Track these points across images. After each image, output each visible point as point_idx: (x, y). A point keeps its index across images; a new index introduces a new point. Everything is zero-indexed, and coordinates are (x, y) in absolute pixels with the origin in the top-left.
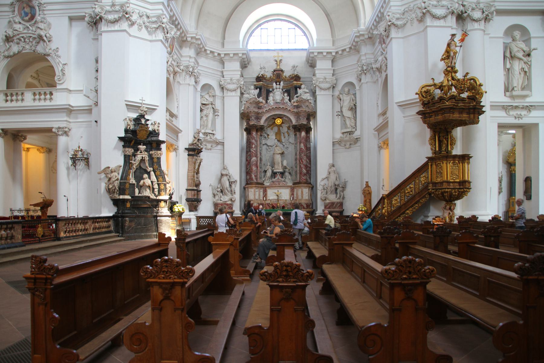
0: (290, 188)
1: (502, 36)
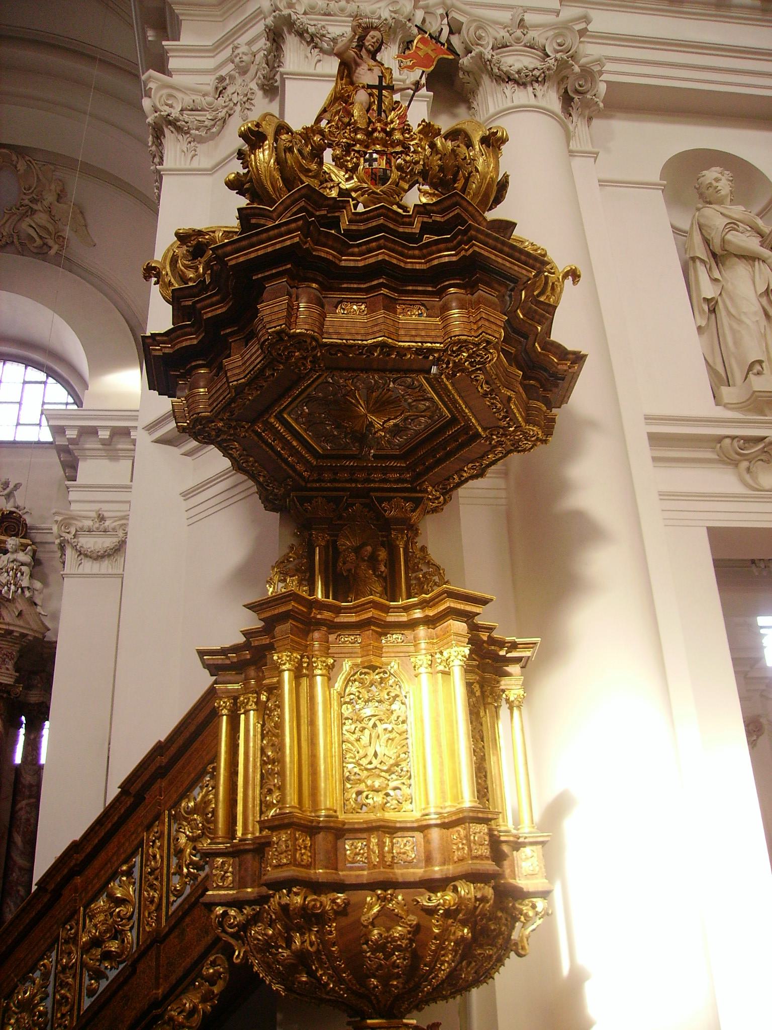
1: (655, 177)
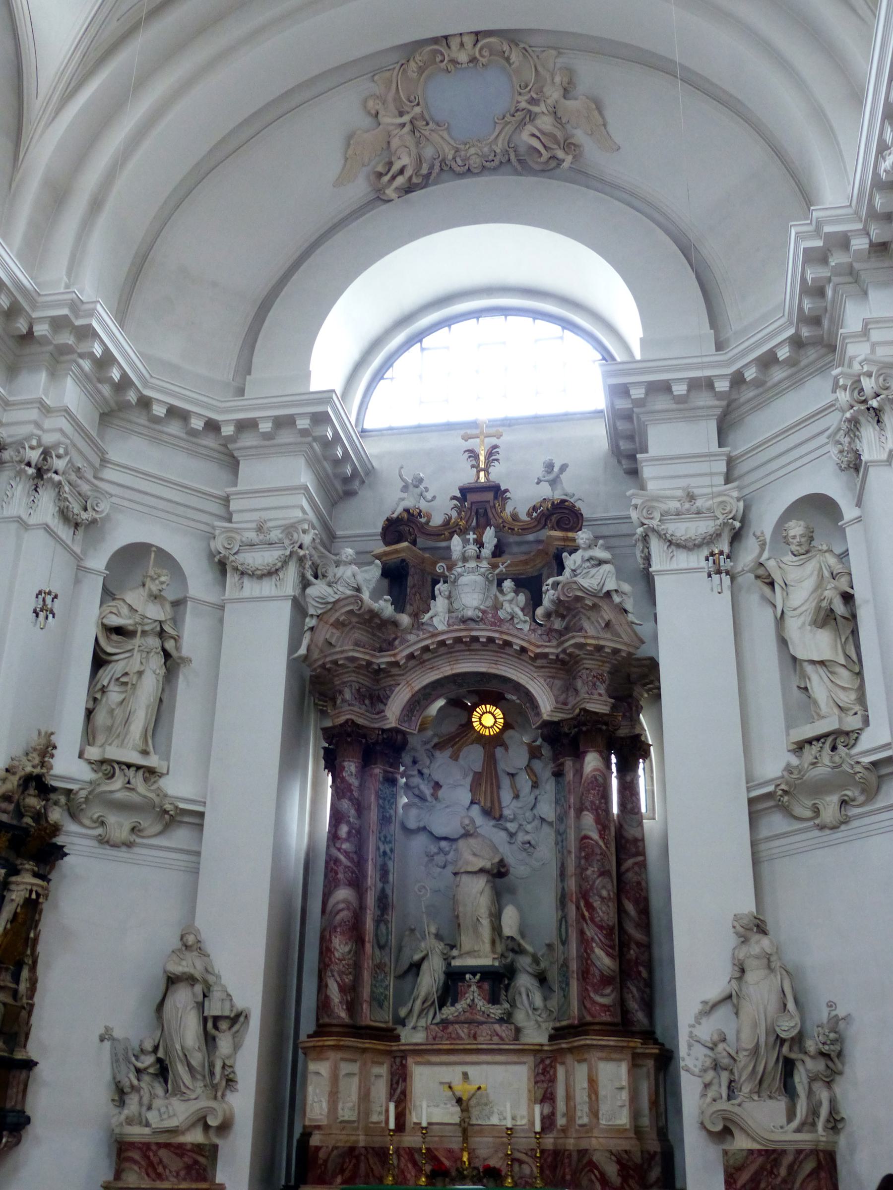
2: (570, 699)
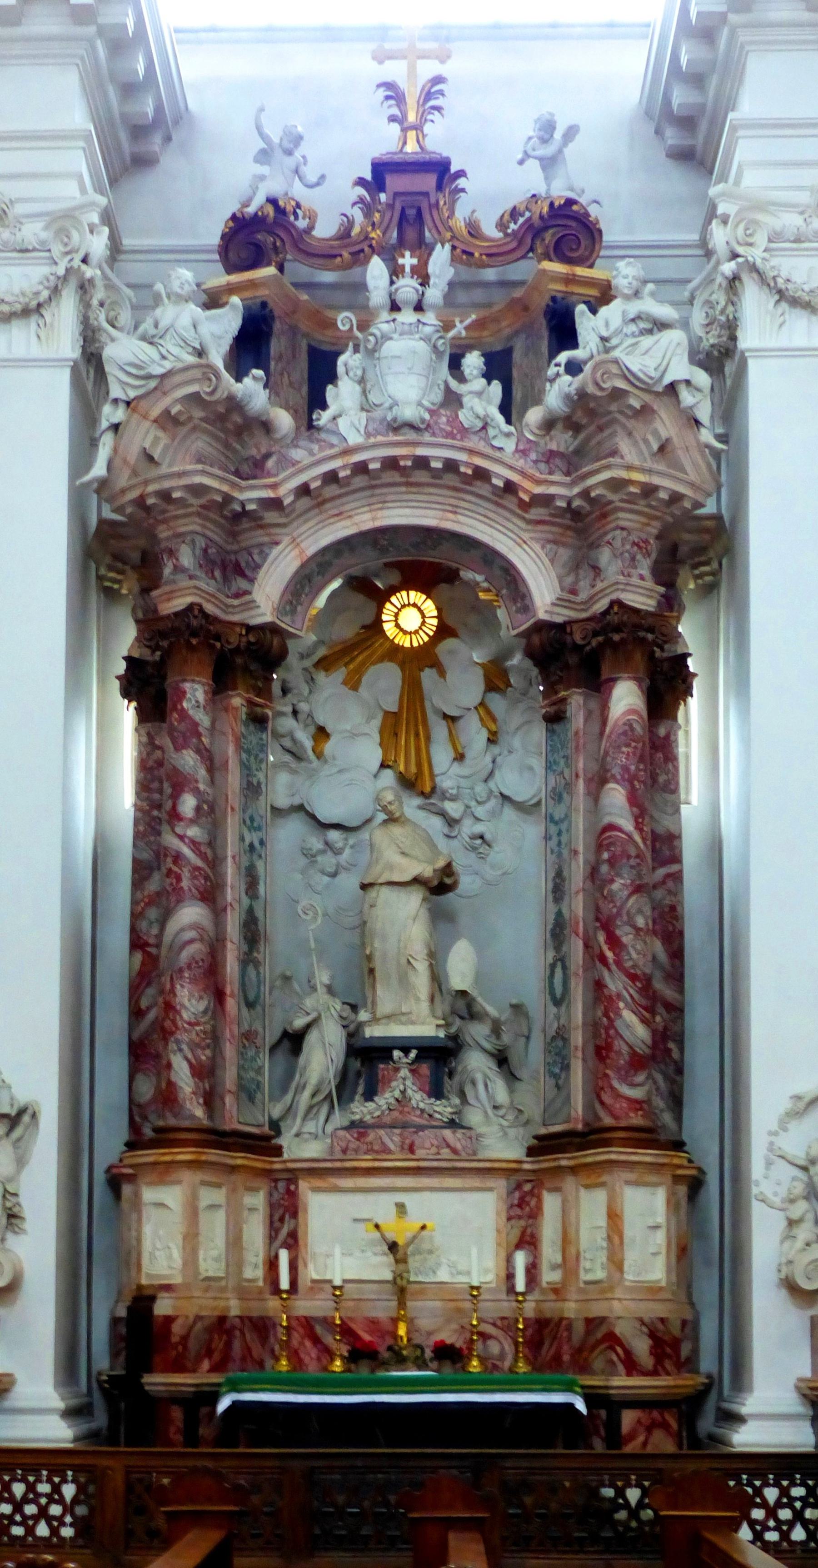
0: (501, 1184)
2: (582, 583)
